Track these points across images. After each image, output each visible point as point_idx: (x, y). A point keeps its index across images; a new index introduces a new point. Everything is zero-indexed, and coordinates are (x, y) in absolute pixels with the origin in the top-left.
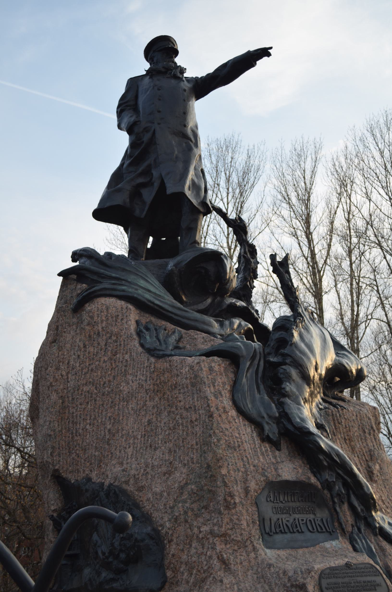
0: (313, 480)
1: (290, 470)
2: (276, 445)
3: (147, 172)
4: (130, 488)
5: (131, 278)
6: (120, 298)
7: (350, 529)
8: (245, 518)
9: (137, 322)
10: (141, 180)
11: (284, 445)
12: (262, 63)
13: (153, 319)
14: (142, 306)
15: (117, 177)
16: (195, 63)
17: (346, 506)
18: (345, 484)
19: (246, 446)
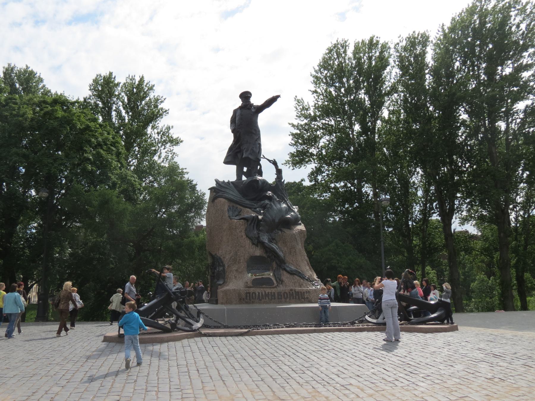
0: (264, 255)
1: (258, 252)
2: (257, 246)
3: (239, 147)
4: (222, 257)
5: (228, 191)
6: (224, 198)
7: (274, 268)
8: (243, 265)
9: (229, 206)
10: (237, 151)
11: (259, 246)
12: (279, 99)
13: (234, 205)
14: (230, 200)
15: (231, 149)
16: (256, 101)
17: (274, 263)
18: (275, 257)
19: (247, 246)
